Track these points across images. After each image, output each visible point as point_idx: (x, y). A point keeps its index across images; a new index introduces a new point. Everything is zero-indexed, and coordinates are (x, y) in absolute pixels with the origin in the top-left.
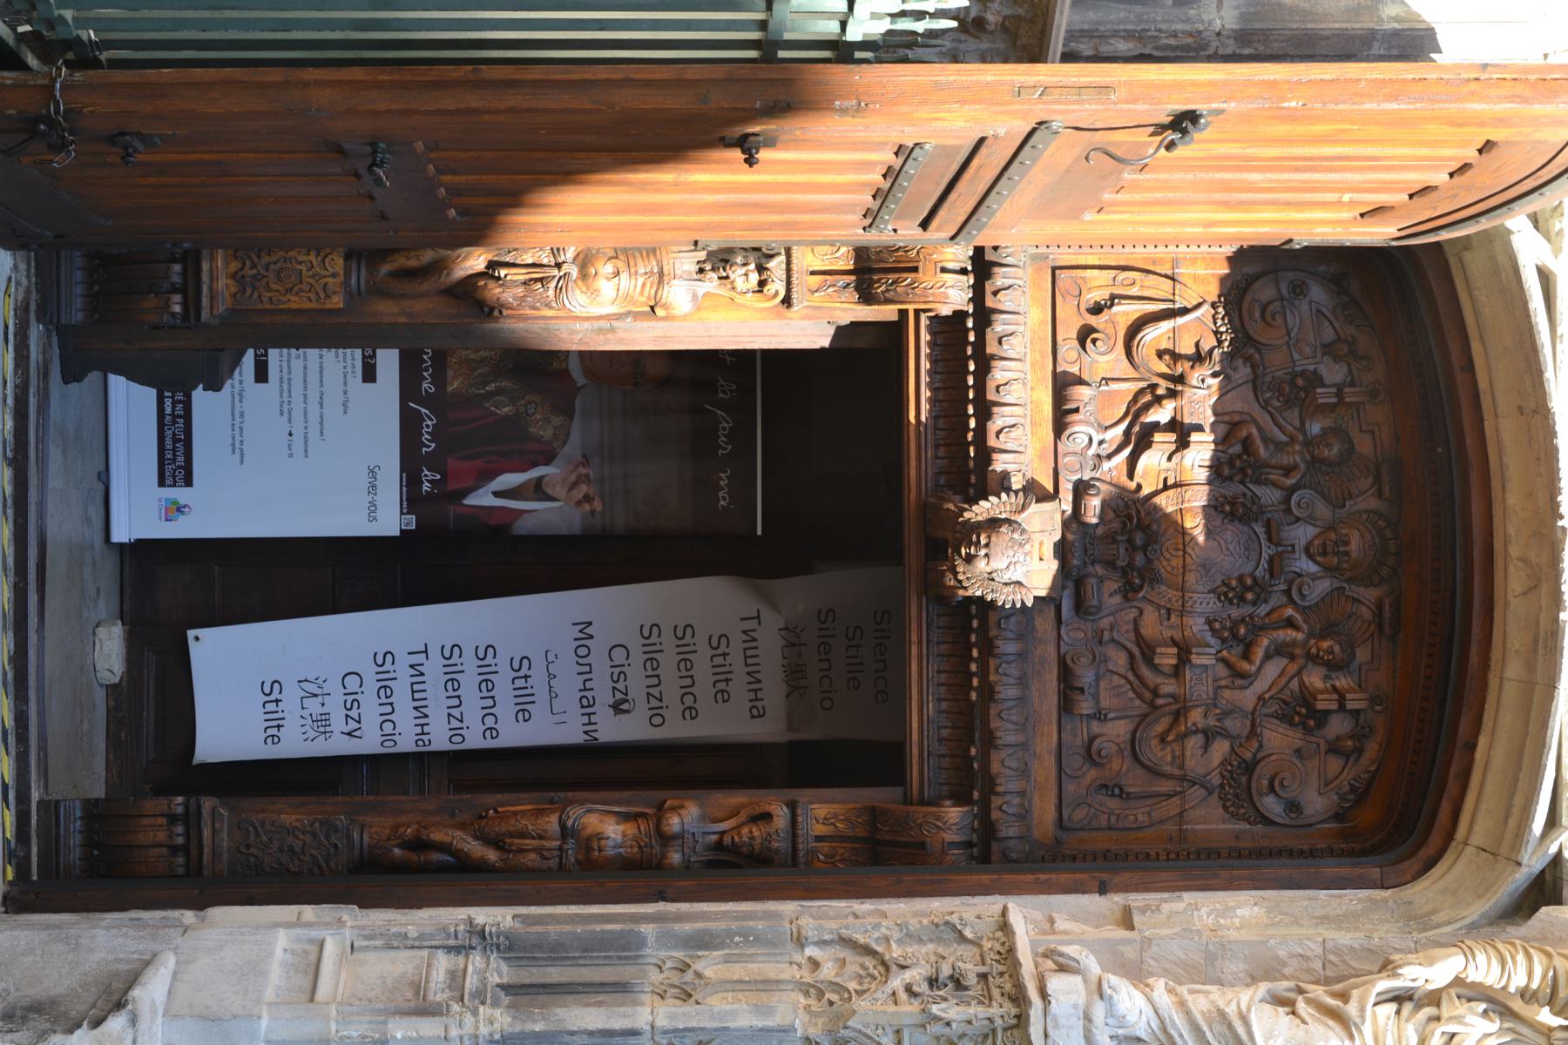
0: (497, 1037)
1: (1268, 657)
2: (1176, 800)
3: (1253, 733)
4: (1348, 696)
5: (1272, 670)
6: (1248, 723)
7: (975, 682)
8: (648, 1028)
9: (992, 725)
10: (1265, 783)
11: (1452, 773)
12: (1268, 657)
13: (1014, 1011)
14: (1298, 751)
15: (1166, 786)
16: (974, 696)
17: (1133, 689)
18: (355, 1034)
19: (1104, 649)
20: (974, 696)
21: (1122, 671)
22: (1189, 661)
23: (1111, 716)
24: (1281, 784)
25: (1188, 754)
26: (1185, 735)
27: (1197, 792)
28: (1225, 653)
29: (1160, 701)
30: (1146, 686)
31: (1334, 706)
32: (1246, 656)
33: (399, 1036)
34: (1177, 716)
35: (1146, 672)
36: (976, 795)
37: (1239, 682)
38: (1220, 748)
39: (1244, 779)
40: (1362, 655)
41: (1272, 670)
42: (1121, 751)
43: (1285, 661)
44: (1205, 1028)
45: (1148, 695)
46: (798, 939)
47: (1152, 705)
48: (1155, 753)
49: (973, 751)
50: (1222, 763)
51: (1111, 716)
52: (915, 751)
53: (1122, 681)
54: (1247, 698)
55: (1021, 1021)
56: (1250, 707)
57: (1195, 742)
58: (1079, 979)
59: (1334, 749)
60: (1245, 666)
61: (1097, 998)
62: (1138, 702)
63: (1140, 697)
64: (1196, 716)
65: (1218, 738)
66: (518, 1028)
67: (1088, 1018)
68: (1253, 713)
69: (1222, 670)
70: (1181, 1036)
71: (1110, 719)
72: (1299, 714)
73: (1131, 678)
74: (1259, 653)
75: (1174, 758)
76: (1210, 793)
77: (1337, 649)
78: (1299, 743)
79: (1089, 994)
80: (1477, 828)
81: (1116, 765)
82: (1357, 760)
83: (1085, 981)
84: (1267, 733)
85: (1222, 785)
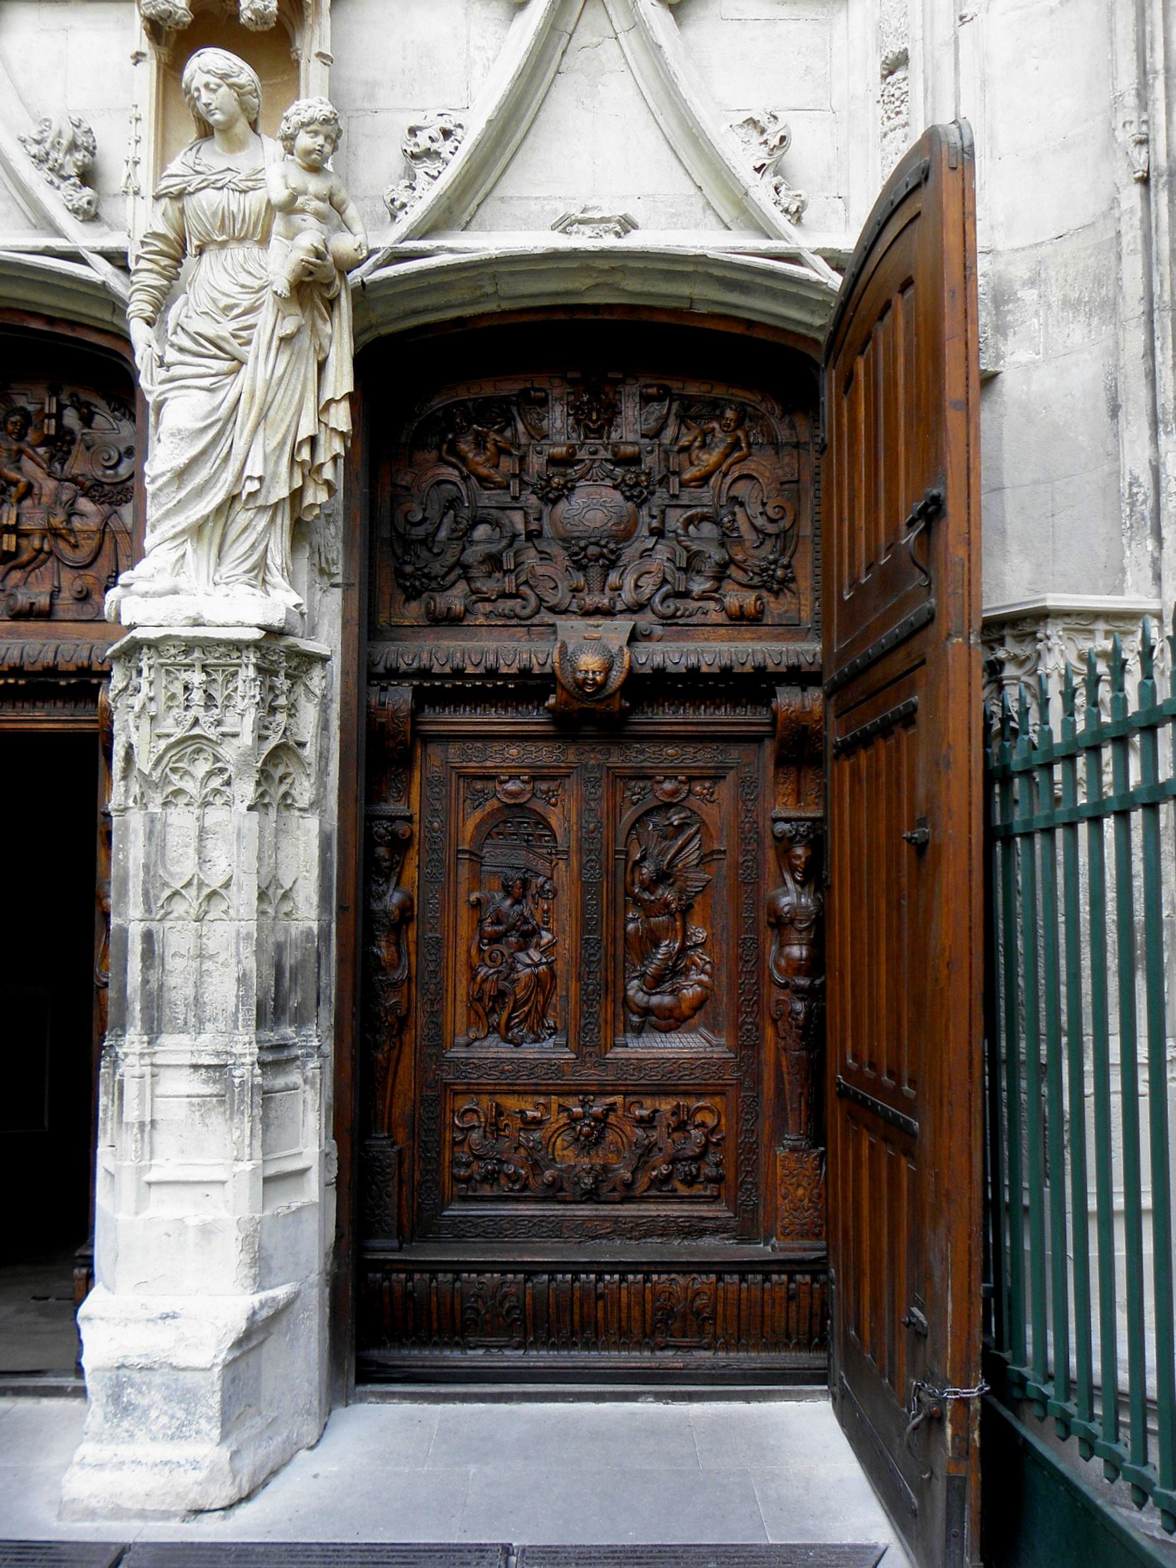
0: (145, 1038)
1: (19, 469)
2: (119, 537)
3: (73, 480)
4: (47, 411)
5: (27, 464)
6: (67, 484)
7: (11, 681)
8: (142, 924)
9: (40, 669)
10: (110, 472)
11: (70, 334)
12: (19, 469)
13: (145, 650)
14: (88, 448)
15: (108, 545)
16: (22, 682)
17: (38, 567)
18: (133, 1147)
19: (8, 588)
20: (22, 682)
21: (25, 575)
22: (13, 526)
23: (56, 584)
24: (107, 460)
25: (85, 528)
26: (71, 531)
27: (113, 523)
28: (13, 500)
29: (46, 547)
30: (35, 558)
31: (53, 422)
32: (15, 483)
33: (137, 1113)
34: (55, 533)
35: (25, 557)
36: (95, 681)
37: (36, 491)
38: (84, 504)
39: (107, 487)
40: (21, 402)
41: (27, 464)
42: (80, 576)
43: (24, 457)
44: (165, 508)
45: (42, 556)
46: (122, 811)
47: (50, 553)
48: (83, 555)
49: (63, 683)
50: (94, 503)
51: (56, 584)
52: (70, 726)
53: (33, 574)
54: (50, 485)
55: (152, 645)
56: (56, 483)
57: (77, 523)
58: (123, 601)
59: (87, 420)
60: (21, 485)
61: (133, 588)
62: (49, 564)
63: (44, 562)
64: (58, 521)
65: (76, 506)
66: (139, 1023)
67: (145, 595)
68: (60, 480)
69: (28, 503)
70: (173, 527)
71: (59, 582)
72: (61, 447)
73: (29, 569)
74: (14, 475)
75: (89, 538)
76: (116, 512)
77: (13, 419)
78: (82, 447)
79: (131, 594)
80: (99, 315)
81: (90, 580)
82: (96, 407)
83: (124, 597)
84: (75, 471)
85: (110, 504)
